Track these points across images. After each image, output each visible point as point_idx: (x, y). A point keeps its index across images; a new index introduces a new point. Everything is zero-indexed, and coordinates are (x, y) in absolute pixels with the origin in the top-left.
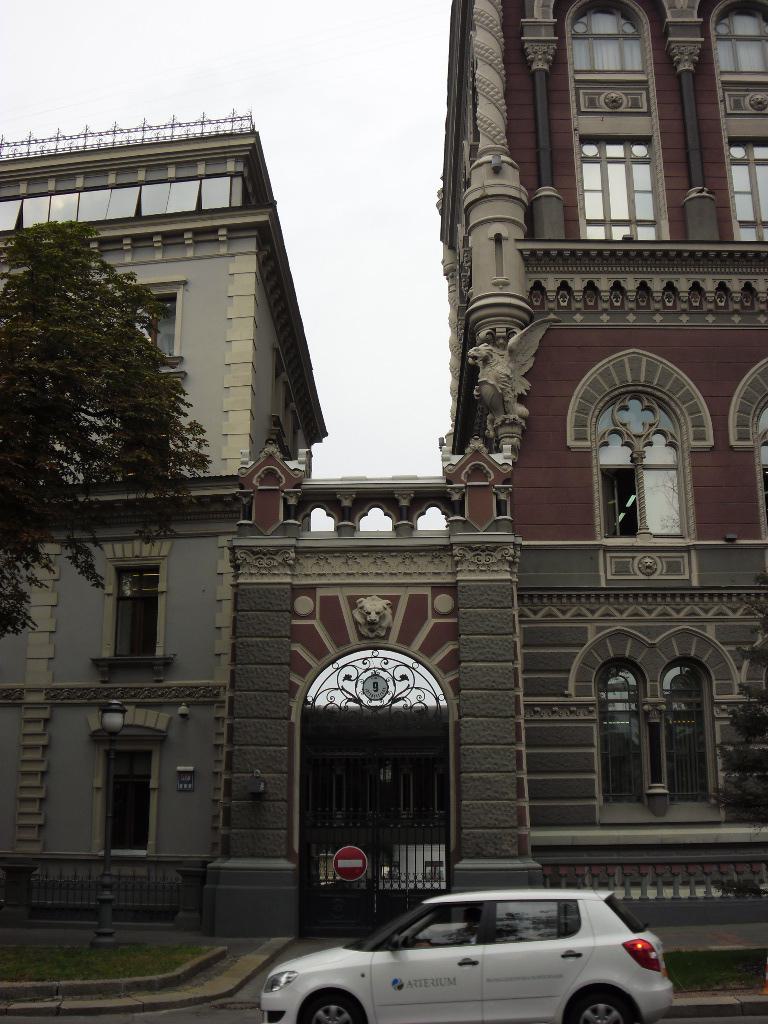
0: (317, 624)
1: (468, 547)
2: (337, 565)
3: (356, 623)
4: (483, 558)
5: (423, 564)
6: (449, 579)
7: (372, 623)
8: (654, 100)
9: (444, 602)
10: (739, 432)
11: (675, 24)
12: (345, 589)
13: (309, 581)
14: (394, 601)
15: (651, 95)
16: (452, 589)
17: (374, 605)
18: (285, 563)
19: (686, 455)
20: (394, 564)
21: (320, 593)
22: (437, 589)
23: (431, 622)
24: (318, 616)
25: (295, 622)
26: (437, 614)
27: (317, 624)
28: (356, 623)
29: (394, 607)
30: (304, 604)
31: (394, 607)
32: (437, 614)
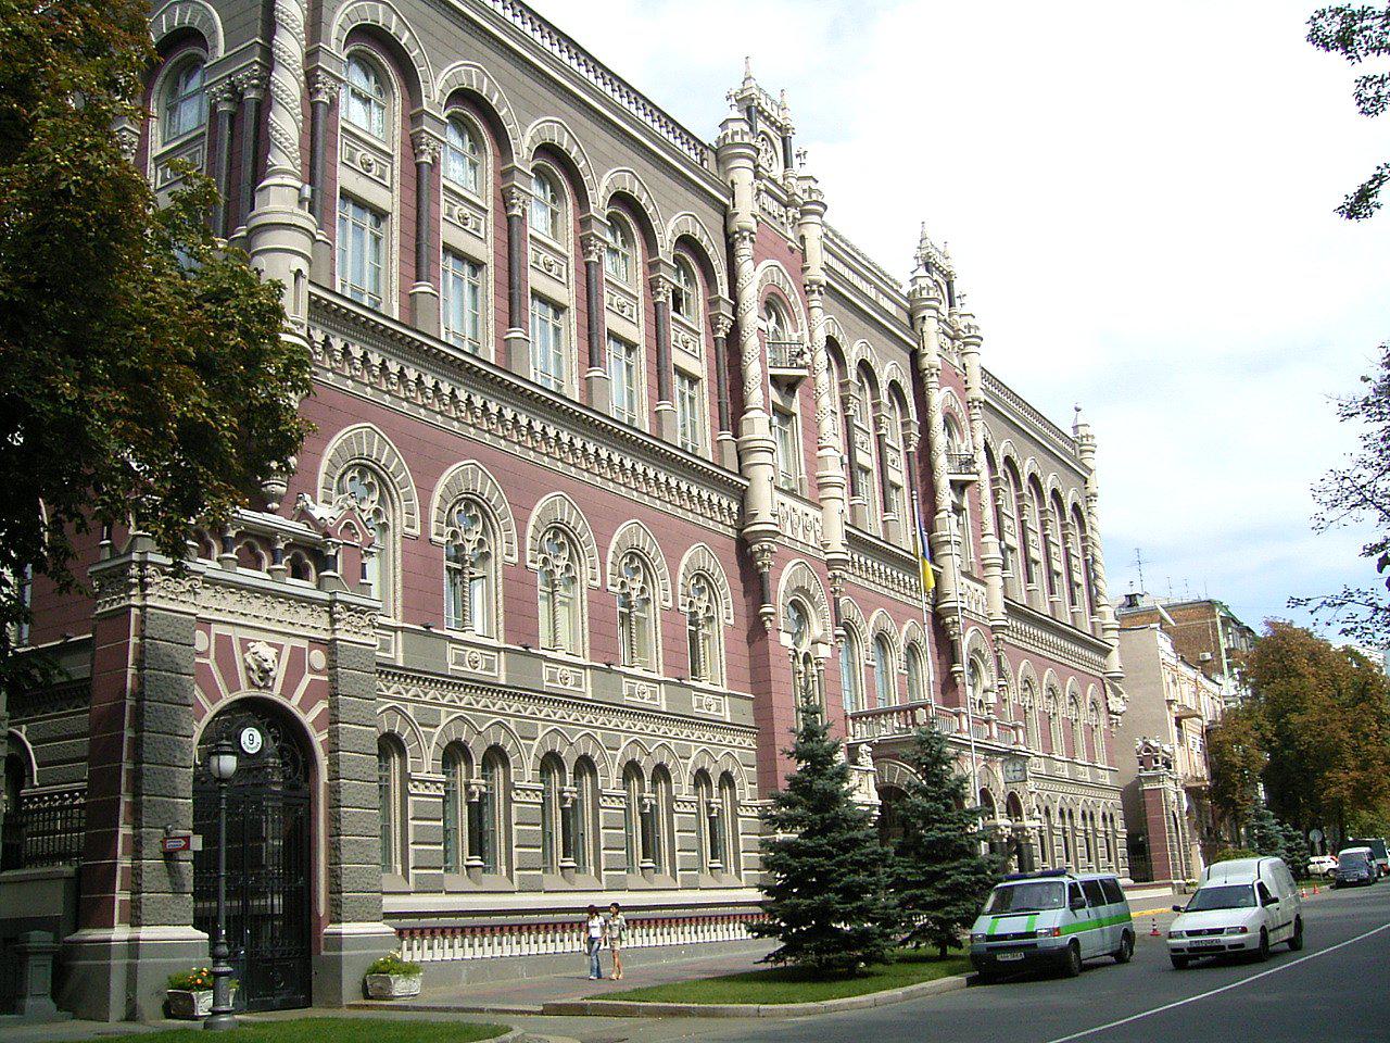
0: (211, 662)
1: (347, 606)
2: (231, 601)
3: (248, 668)
4: (355, 620)
5: (303, 615)
6: (327, 636)
7: (266, 672)
8: (397, 178)
9: (318, 658)
10: (438, 527)
11: (428, 114)
12: (237, 629)
13: (203, 614)
14: (279, 647)
15: (395, 172)
16: (330, 647)
17: (270, 653)
18: (193, 591)
19: (398, 538)
20: (280, 610)
21: (216, 629)
22: (314, 642)
23: (308, 678)
24: (212, 656)
25: (197, 660)
26: (314, 671)
27: (211, 662)
28: (248, 668)
29: (278, 655)
30: (202, 641)
31: (278, 655)
32: (314, 671)
